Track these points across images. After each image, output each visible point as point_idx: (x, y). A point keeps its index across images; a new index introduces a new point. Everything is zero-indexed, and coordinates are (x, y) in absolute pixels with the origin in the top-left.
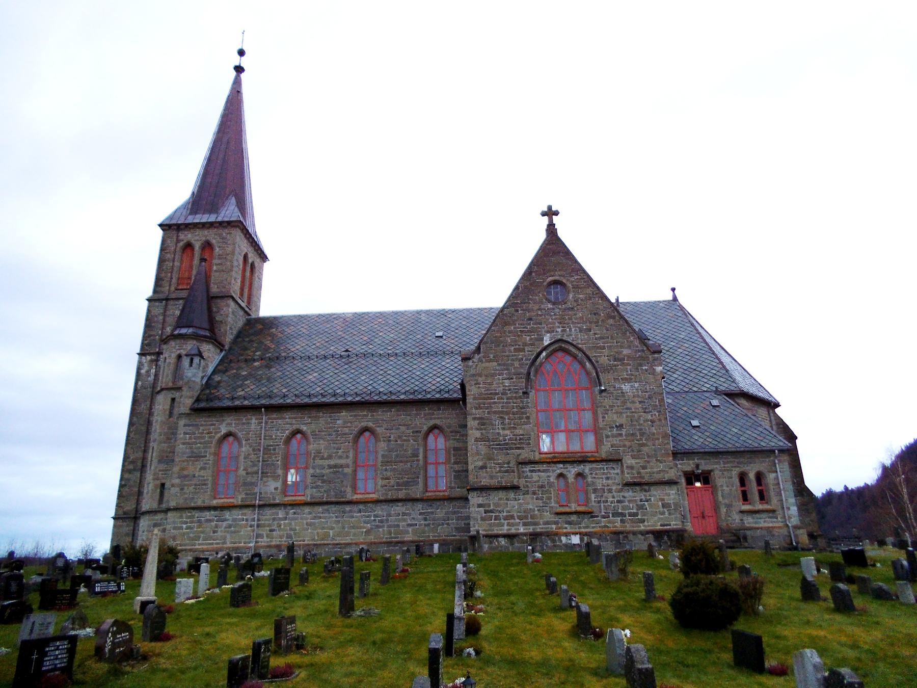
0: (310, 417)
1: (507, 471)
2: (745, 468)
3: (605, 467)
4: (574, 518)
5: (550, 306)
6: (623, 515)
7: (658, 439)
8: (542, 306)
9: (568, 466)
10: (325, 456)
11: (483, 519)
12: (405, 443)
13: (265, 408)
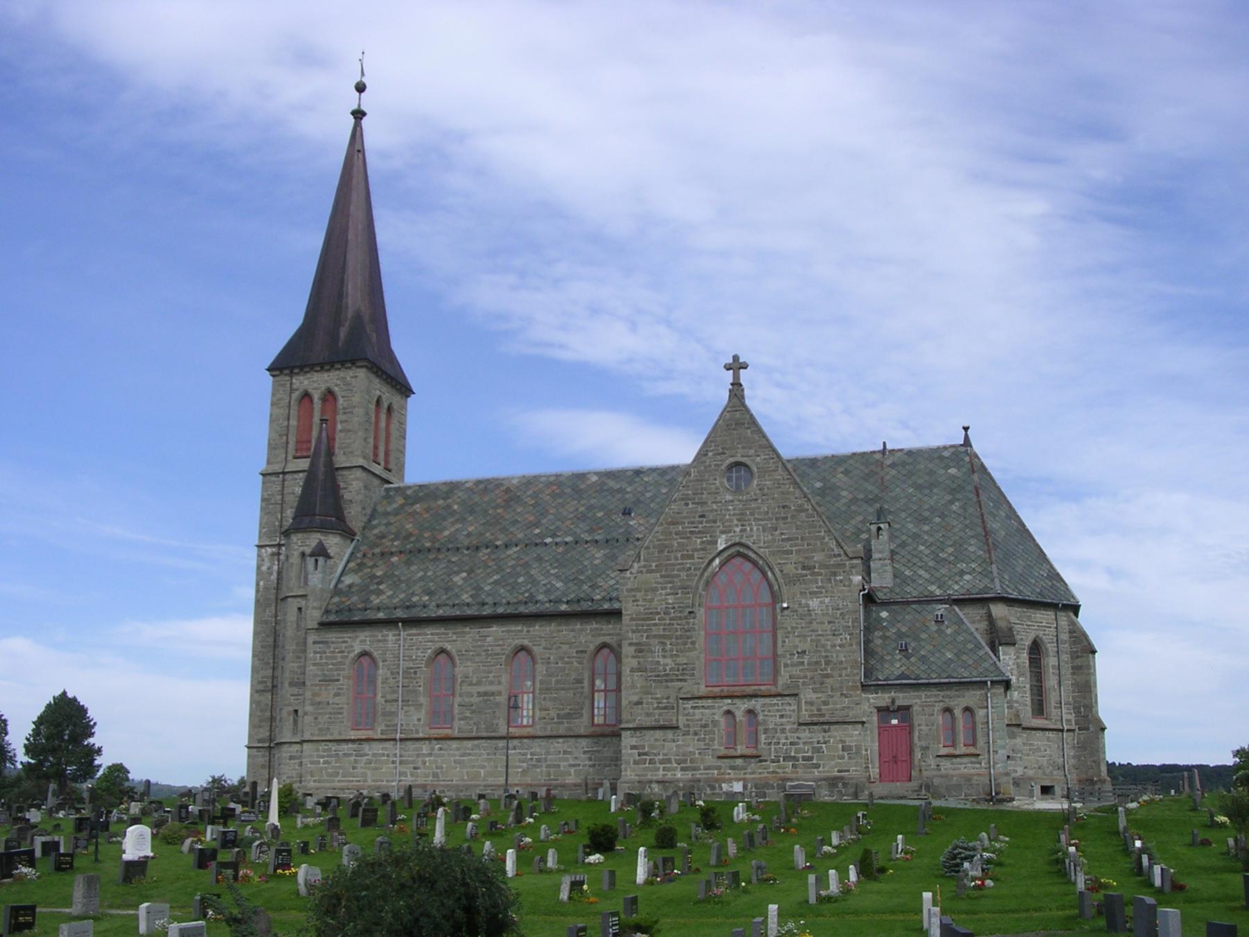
0: (454, 633)
1: (665, 708)
2: (952, 704)
3: (780, 703)
4: (739, 762)
5: (729, 497)
6: (797, 759)
7: (846, 669)
8: (719, 499)
9: (736, 701)
10: (474, 682)
11: (636, 763)
12: (567, 666)
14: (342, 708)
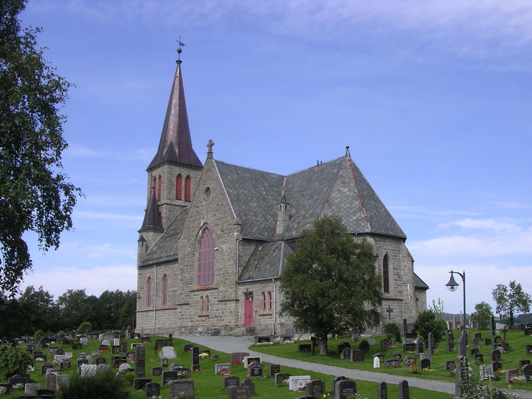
4: (204, 318)
13: (155, 264)
14: (144, 299)
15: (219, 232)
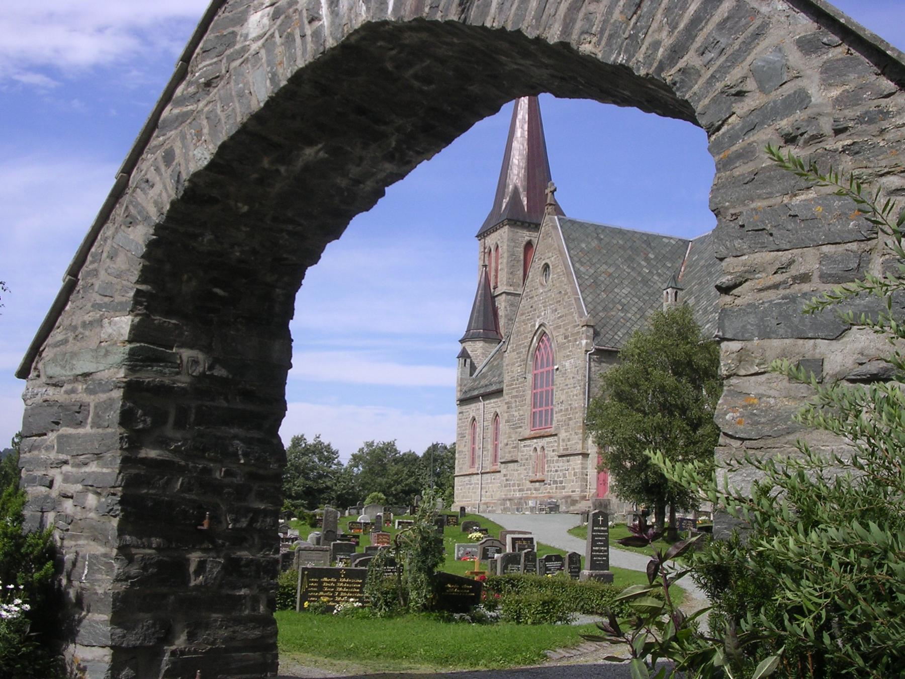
15: (561, 339)
